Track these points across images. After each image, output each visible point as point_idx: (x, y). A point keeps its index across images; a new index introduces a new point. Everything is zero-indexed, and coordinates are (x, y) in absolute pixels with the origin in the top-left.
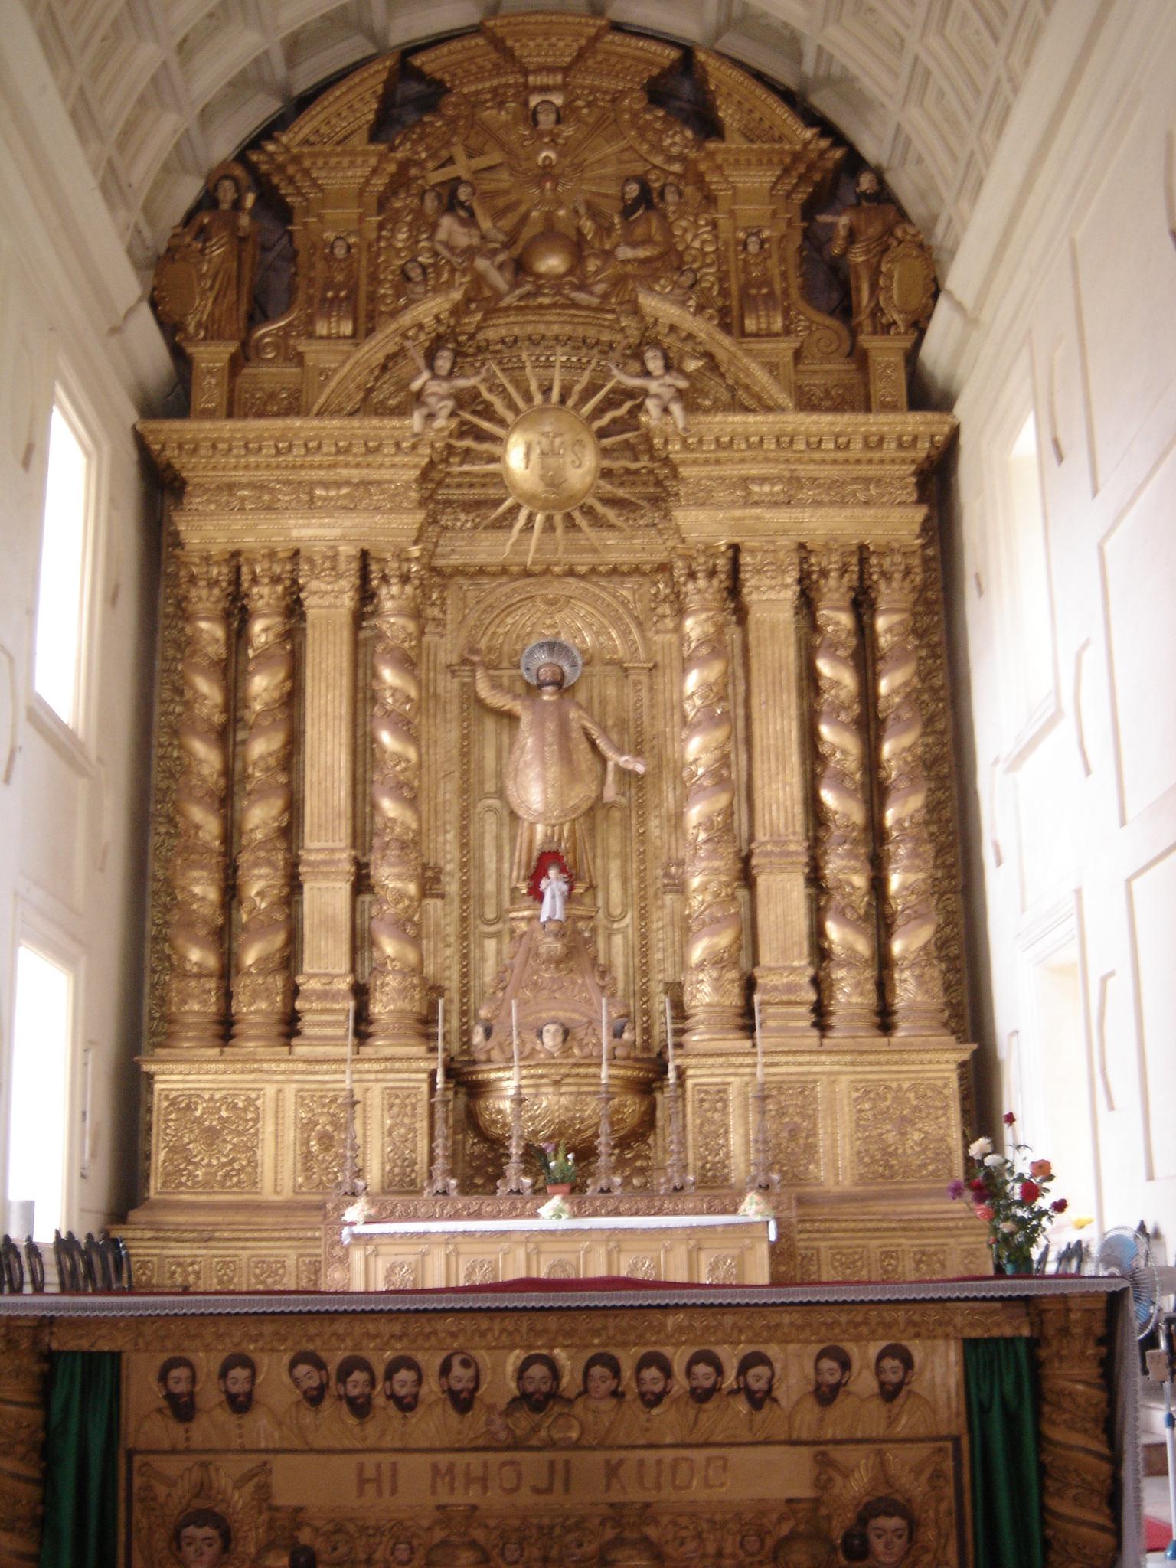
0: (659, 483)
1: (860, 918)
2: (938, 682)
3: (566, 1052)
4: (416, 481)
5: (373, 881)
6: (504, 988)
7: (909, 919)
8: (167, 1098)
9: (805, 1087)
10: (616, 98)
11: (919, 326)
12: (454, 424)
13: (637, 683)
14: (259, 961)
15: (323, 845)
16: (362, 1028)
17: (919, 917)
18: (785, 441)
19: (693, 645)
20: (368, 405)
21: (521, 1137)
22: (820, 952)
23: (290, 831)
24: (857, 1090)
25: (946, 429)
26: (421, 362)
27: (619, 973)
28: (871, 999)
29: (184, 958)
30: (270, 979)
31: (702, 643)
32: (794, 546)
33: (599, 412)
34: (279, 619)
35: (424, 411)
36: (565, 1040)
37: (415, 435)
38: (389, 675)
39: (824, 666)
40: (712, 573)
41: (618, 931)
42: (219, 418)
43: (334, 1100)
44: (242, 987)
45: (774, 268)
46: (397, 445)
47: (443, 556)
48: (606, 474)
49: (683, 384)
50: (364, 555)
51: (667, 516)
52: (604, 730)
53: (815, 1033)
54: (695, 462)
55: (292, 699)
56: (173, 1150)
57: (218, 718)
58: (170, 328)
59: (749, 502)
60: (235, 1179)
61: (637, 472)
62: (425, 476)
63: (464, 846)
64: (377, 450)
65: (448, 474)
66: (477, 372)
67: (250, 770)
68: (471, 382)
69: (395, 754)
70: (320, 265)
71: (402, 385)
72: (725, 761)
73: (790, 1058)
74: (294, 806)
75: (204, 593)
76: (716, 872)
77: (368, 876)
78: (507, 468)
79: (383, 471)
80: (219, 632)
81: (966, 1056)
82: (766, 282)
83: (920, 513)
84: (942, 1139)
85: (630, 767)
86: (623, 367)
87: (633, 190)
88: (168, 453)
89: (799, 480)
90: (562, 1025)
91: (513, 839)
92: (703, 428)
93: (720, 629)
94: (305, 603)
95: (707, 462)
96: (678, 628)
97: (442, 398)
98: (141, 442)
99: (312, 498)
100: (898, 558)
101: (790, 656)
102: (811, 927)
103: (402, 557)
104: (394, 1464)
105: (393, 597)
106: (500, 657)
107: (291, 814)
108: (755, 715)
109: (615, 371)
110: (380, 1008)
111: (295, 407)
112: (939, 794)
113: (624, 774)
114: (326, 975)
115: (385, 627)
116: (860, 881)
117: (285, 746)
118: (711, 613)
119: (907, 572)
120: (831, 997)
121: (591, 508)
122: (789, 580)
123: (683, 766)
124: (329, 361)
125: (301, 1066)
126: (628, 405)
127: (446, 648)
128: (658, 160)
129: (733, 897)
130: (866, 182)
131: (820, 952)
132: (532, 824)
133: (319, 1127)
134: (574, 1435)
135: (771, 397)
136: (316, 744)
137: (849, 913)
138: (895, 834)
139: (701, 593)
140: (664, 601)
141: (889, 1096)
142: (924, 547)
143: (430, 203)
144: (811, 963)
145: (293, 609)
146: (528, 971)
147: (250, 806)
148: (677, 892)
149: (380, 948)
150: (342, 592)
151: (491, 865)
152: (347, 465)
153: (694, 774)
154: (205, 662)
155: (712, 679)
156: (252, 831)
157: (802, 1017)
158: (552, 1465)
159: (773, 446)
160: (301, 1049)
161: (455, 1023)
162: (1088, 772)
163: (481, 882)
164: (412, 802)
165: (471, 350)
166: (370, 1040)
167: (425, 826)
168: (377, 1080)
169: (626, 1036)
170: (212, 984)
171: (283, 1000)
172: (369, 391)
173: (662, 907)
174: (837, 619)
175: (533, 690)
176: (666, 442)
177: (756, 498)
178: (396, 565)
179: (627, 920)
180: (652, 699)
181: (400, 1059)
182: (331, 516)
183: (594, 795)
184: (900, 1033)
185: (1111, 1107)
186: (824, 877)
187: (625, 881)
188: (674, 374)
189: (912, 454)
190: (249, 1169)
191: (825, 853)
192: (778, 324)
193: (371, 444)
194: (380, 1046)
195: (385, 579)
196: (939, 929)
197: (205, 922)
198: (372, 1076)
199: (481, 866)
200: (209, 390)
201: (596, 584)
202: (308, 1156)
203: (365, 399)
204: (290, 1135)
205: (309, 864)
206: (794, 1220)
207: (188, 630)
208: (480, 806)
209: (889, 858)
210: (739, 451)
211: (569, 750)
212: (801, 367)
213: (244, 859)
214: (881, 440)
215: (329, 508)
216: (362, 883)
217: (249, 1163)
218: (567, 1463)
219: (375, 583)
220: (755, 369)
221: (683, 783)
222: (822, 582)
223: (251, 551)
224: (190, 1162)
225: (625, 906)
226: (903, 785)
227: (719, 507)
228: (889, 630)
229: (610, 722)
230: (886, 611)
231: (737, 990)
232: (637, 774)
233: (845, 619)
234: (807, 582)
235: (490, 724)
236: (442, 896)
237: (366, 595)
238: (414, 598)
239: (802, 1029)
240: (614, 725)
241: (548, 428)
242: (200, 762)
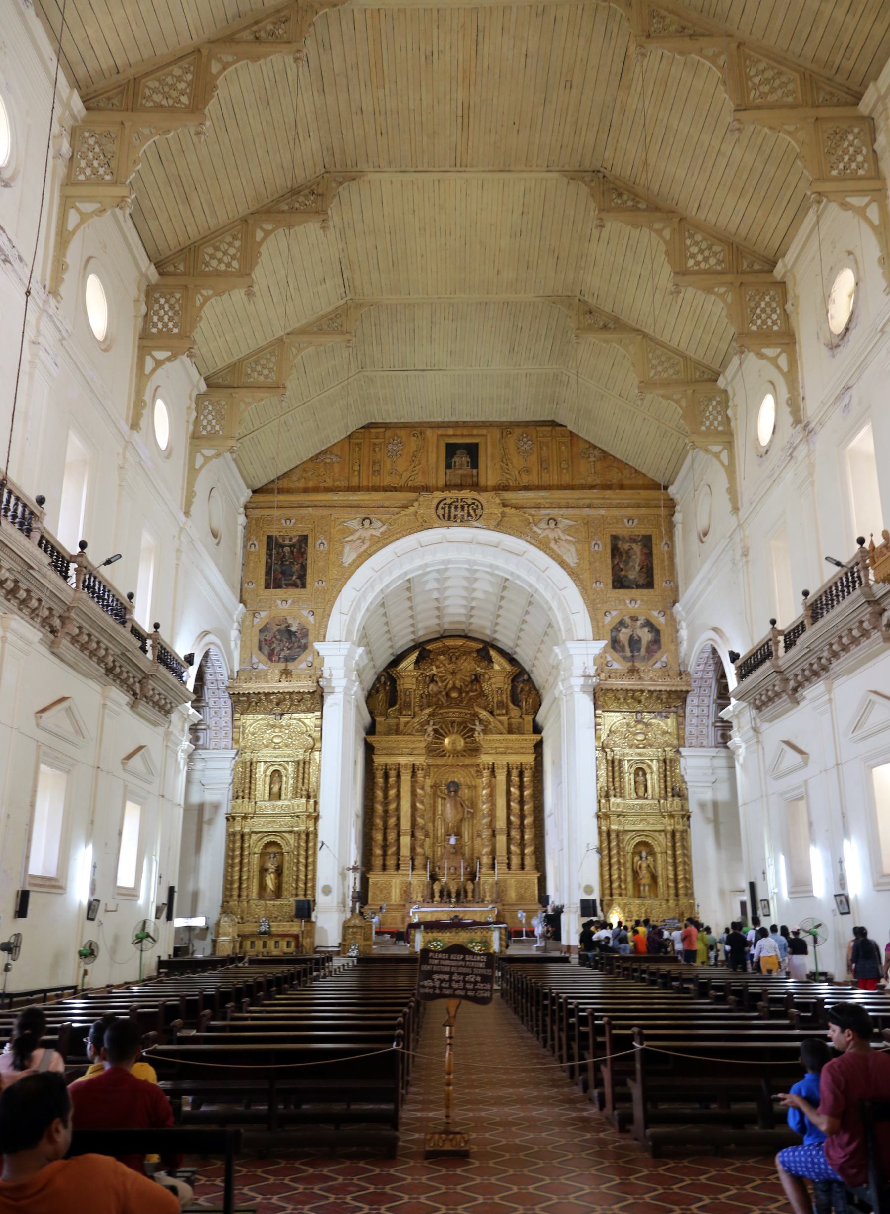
9: (505, 881)
10: (470, 653)
11: (536, 712)
17: (531, 845)
22: (509, 852)
23: (398, 825)
27: (467, 856)
39: (512, 789)
40: (488, 769)
44: (388, 858)
45: (504, 696)
50: (414, 765)
55: (398, 795)
56: (374, 893)
58: (371, 712)
70: (403, 696)
74: (398, 819)
82: (502, 702)
83: (534, 756)
87: (473, 677)
101: (505, 787)
103: (421, 764)
110: (416, 863)
111: (397, 732)
113: (468, 812)
116: (518, 837)
127: (429, 782)
128: (478, 669)
130: (526, 677)
139: (486, 773)
143: (427, 679)
145: (398, 776)
157: (505, 867)
160: (400, 872)
164: (423, 819)
170: (381, 858)
174: (515, 779)
192: (504, 711)
204: (398, 891)
213: (388, 831)
216: (413, 835)
233: (517, 779)
235: (440, 800)
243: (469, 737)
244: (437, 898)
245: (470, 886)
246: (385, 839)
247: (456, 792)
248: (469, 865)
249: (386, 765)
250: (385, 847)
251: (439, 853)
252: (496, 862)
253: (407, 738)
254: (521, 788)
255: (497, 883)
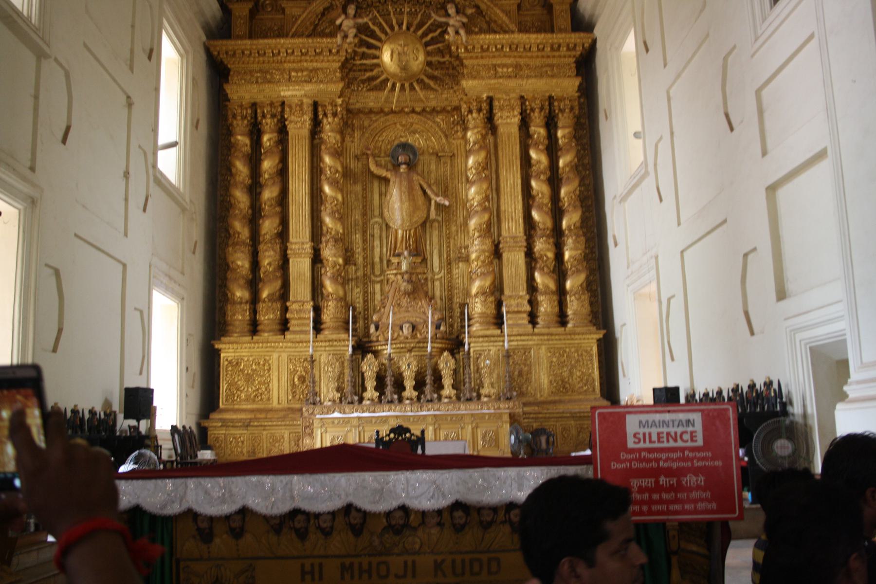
0: (454, 68)
1: (550, 271)
2: (586, 161)
3: (414, 336)
4: (339, 68)
5: (322, 257)
6: (384, 307)
7: (573, 273)
8: (227, 360)
9: (526, 350)
12: (356, 40)
13: (445, 163)
14: (268, 296)
15: (298, 240)
16: (318, 327)
18: (514, 47)
19: (471, 145)
20: (315, 33)
21: (393, 376)
22: (532, 287)
23: (283, 235)
24: (550, 352)
25: (590, 41)
26: (340, 10)
28: (557, 309)
29: (233, 294)
30: (274, 304)
31: (475, 143)
32: (518, 97)
33: (425, 34)
34: (275, 135)
35: (342, 34)
36: (413, 331)
37: (338, 46)
38: (327, 160)
39: (533, 154)
40: (479, 110)
41: (437, 279)
42: (245, 38)
43: (306, 360)
44: (261, 306)
46: (330, 51)
47: (353, 104)
48: (429, 64)
49: (465, 20)
50: (315, 105)
51: (458, 83)
52: (430, 186)
53: (530, 326)
54: (471, 58)
55: (283, 172)
57: (248, 181)
59: (496, 76)
60: (260, 398)
61: (444, 63)
62: (343, 66)
63: (365, 241)
64: (321, 53)
65: (354, 65)
66: (368, 15)
67: (263, 206)
68: (366, 20)
69: (331, 197)
71: (332, 22)
72: (487, 198)
73: (519, 338)
74: (284, 222)
75: (240, 122)
76: (483, 251)
77: (319, 255)
78: (382, 60)
79: (323, 64)
80: (248, 141)
81: (601, 336)
83: (577, 82)
84: (590, 375)
85: (442, 202)
86: (436, 13)
88: (221, 56)
89: (520, 66)
90: (412, 324)
91: (387, 237)
92: (475, 42)
93: (484, 137)
94: (288, 127)
95: (477, 58)
96: (464, 137)
97: (350, 28)
98: (208, 51)
99: (290, 77)
100: (567, 102)
102: (527, 276)
104: (321, 565)
105: (329, 123)
106: (380, 151)
107: (283, 226)
108: (502, 178)
109: (433, 15)
110: (327, 316)
111: (281, 33)
112: (587, 214)
113: (438, 206)
114: (300, 301)
115: (325, 137)
116: (550, 255)
117: (279, 195)
118: (479, 129)
119: (572, 109)
120: (537, 309)
121: (422, 81)
122: (516, 113)
123: (467, 201)
124: (296, 11)
125: (289, 344)
126: (439, 31)
129: (491, 263)
131: (532, 287)
132: (396, 231)
133: (299, 373)
134: (417, 547)
135: (507, 26)
136: (294, 194)
137: (546, 270)
138: (567, 232)
139: (475, 120)
140: (457, 124)
141: (565, 355)
142: (579, 97)
144: (528, 293)
145: (282, 131)
146: (396, 298)
147: (264, 222)
148: (465, 261)
149: (325, 288)
150: (305, 121)
151: (377, 250)
152: (306, 61)
153: (472, 205)
154: (241, 155)
155: (480, 160)
156: (265, 234)
157: (524, 320)
158: (406, 563)
159: (508, 50)
160: (289, 336)
161: (361, 323)
162: (661, 200)
163: (373, 258)
165: (365, 6)
166: (322, 332)
167: (346, 231)
168: (325, 351)
169: (442, 328)
171: (281, 314)
172: (317, 25)
173: (458, 268)
174: (538, 131)
175: (396, 166)
176: (457, 48)
177: (500, 74)
178: (330, 108)
179: (442, 274)
180: (452, 170)
181: (336, 341)
182: (299, 85)
183: (425, 216)
184: (570, 325)
185: (673, 359)
186: (534, 253)
187: (440, 256)
188: (461, 15)
189: (573, 53)
190: (266, 393)
191: (534, 241)
193: (317, 51)
194: (326, 334)
195: (325, 115)
196: (587, 277)
197: (243, 277)
198: (323, 349)
199: (372, 249)
200: (240, 25)
201: (425, 117)
202: (293, 385)
203: (314, 30)
204: (285, 377)
205: (291, 249)
206: (521, 414)
207: (233, 140)
208: (372, 222)
209: (564, 245)
210: (492, 52)
211: (413, 196)
212: (521, 12)
213: (262, 247)
214: (559, 46)
215: (298, 82)
216: (317, 259)
217: (266, 390)
218: (414, 562)
219: (321, 117)
220: (498, 11)
221: (467, 210)
222: (532, 114)
223: (262, 103)
224: (238, 390)
225: (441, 268)
226: (571, 209)
227: (483, 78)
228: (564, 136)
229: (432, 182)
230: (564, 127)
231: (494, 306)
232: (445, 206)
233: (542, 131)
234: (524, 114)
235: (376, 184)
236: (355, 265)
237: (316, 124)
238: (339, 124)
239: (524, 325)
240: (434, 183)
241: (402, 42)
242: (239, 202)
243: (433, 41)
244: (371, 393)
245: (446, 364)
246: (255, 265)
247: (411, 166)
248: (443, 319)
249: (254, 106)
250: (254, 284)
251: (378, 297)
252: (504, 309)
253: (298, 41)
254: (552, 150)
255: (508, 355)
